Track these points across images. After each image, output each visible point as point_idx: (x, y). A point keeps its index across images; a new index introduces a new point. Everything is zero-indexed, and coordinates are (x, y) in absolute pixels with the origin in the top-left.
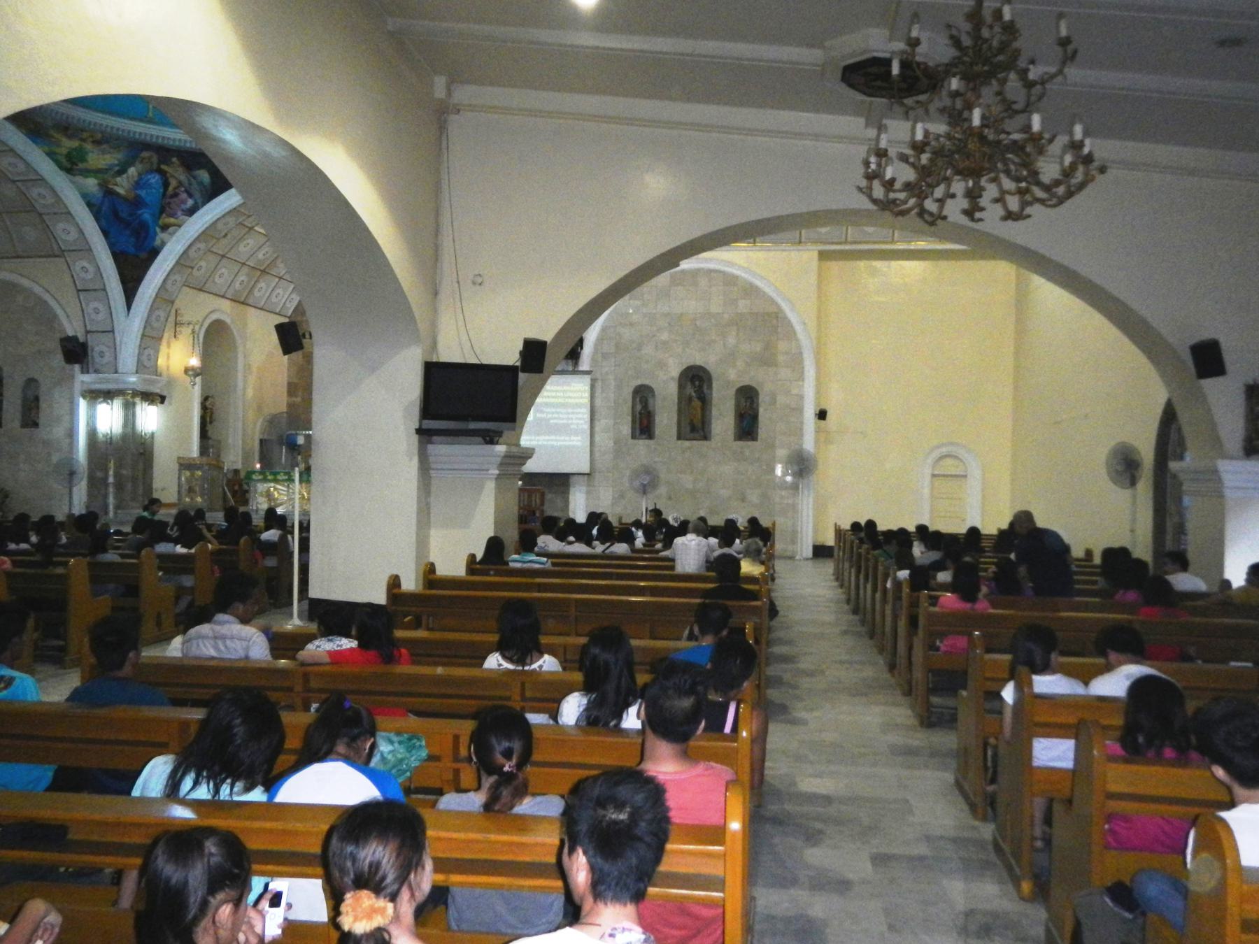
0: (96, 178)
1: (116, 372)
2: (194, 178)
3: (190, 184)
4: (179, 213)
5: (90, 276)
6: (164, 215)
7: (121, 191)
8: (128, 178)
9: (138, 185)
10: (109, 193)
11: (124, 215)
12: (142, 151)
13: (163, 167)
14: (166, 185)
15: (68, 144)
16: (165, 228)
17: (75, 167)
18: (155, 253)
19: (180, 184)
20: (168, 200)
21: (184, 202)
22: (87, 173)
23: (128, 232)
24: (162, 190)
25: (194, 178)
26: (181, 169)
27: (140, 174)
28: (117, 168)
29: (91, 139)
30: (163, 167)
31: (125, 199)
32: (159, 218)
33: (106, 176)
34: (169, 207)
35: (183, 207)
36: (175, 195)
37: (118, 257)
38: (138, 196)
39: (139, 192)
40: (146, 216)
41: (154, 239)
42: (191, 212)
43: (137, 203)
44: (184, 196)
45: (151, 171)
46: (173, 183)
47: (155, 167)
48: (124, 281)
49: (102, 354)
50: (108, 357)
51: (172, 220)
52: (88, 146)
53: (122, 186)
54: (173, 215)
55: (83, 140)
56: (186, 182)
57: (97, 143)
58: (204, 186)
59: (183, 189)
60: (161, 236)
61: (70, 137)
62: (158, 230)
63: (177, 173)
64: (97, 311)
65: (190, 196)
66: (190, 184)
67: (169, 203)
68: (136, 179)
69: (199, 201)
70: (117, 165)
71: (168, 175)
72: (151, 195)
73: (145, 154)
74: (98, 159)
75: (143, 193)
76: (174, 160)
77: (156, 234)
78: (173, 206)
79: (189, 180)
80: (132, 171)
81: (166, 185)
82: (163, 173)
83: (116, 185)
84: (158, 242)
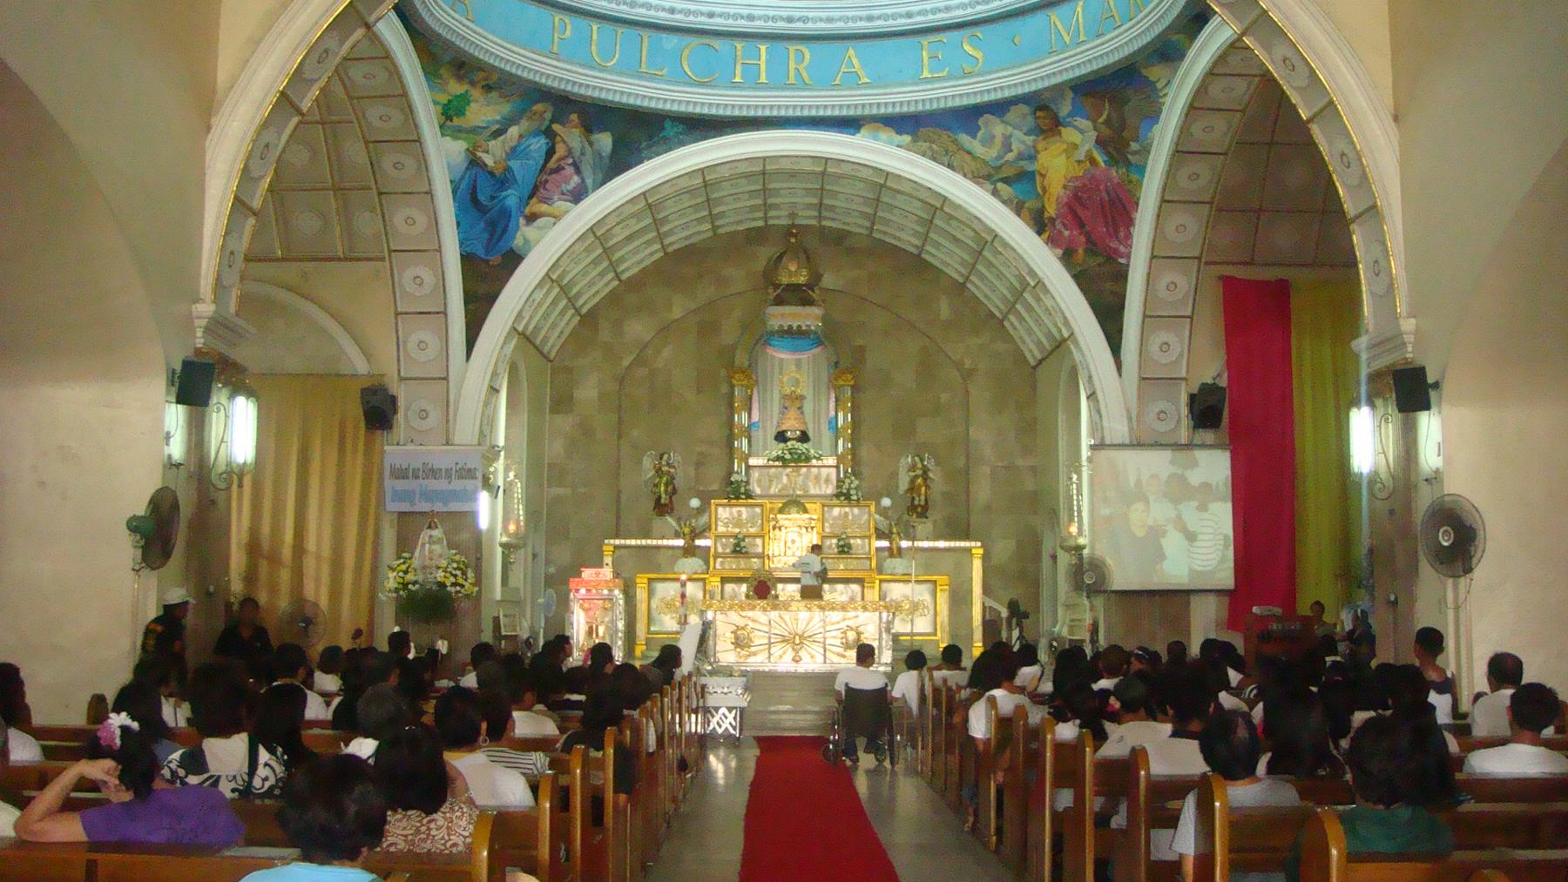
0: (464, 139)
1: (447, 444)
2: (591, 144)
3: (583, 154)
4: (556, 197)
5: (427, 289)
6: (534, 200)
7: (489, 161)
8: (503, 142)
9: (513, 152)
10: (474, 163)
11: (481, 197)
12: (536, 103)
13: (556, 127)
14: (550, 152)
15: (456, 88)
16: (532, 218)
17: (449, 123)
18: (513, 260)
19: (570, 152)
20: (545, 177)
21: (567, 182)
22: (457, 133)
23: (482, 225)
24: (542, 162)
25: (591, 144)
26: (577, 132)
27: (521, 136)
28: (498, 126)
29: (484, 83)
30: (556, 127)
31: (491, 173)
32: (527, 204)
33: (478, 138)
34: (545, 188)
35: (565, 187)
36: (558, 170)
37: (467, 259)
38: (508, 169)
39: (512, 163)
40: (511, 198)
41: (514, 238)
42: (578, 196)
43: (503, 180)
44: (570, 170)
45: (536, 134)
46: (560, 150)
47: (543, 128)
48: (469, 298)
49: (424, 414)
50: (435, 417)
51: (544, 208)
52: (476, 93)
53: (492, 156)
54: (545, 200)
55: (472, 83)
56: (577, 154)
57: (488, 88)
58: (601, 157)
59: (570, 161)
60: (525, 232)
61: (460, 78)
62: (522, 221)
63: (571, 136)
64: (422, 345)
65: (578, 171)
66: (583, 154)
67: (546, 181)
68: (513, 144)
69: (589, 182)
70: (497, 122)
71: (558, 139)
72: (524, 171)
73: (539, 107)
74: (484, 111)
75: (514, 164)
76: (574, 117)
77: (518, 228)
78: (548, 186)
79: (583, 148)
80: (514, 131)
81: (550, 152)
82: (550, 134)
83: (487, 152)
84: (518, 242)
